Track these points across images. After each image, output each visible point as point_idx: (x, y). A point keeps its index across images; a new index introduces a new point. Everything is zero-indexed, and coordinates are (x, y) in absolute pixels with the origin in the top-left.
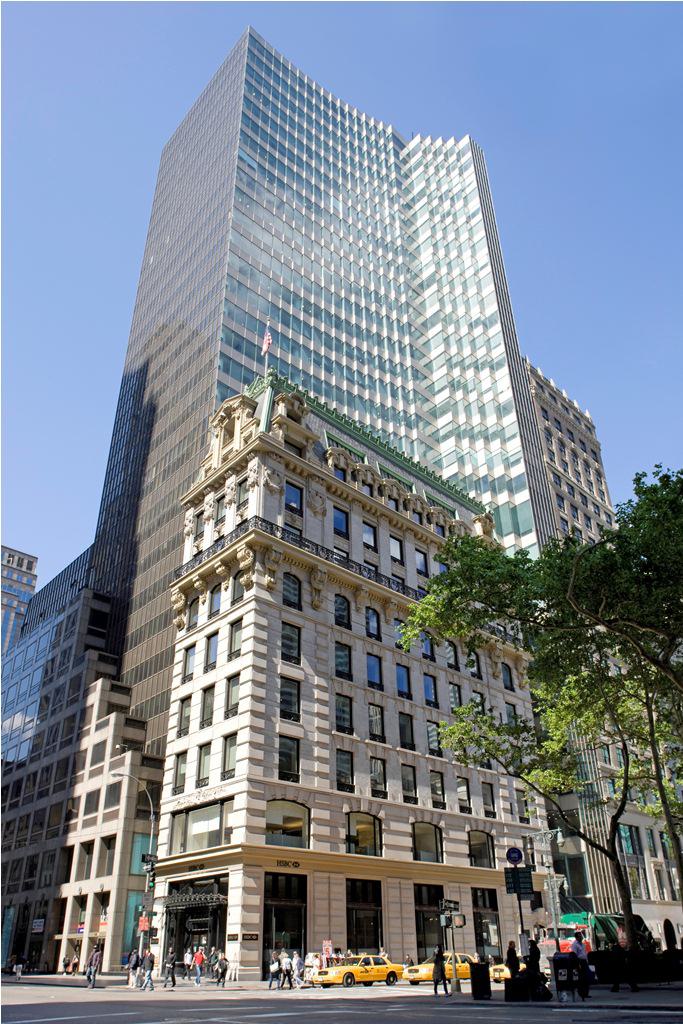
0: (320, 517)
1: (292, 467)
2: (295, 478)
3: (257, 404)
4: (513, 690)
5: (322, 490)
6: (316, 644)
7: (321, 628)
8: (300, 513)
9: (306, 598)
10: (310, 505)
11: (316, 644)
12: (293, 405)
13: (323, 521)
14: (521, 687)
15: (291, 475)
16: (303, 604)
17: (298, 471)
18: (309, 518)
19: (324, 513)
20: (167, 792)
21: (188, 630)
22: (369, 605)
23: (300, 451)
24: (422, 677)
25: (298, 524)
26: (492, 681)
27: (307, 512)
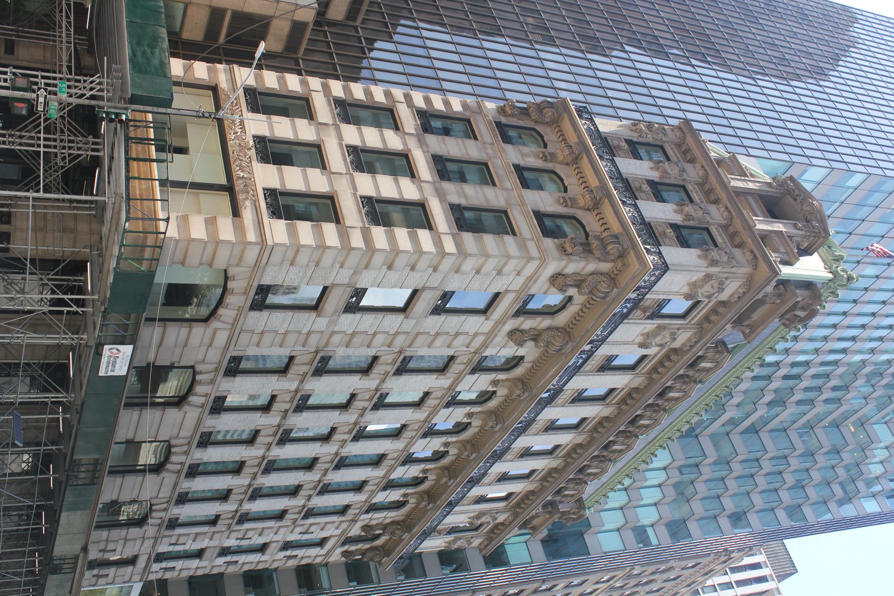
0: (640, 339)
1: (721, 310)
2: (704, 311)
3: (811, 254)
4: (344, 544)
5: (677, 344)
6: (457, 334)
7: (479, 341)
8: (652, 317)
9: (528, 324)
10: (660, 328)
11: (457, 334)
12: (803, 308)
13: (632, 343)
14: (345, 554)
15: (707, 308)
16: (521, 319)
17: (713, 318)
18: (642, 327)
19: (642, 345)
20: (245, 76)
21: (499, 125)
22: (498, 394)
23: (738, 322)
24: (381, 452)
25: (638, 313)
26: (359, 524)
27: (650, 325)
